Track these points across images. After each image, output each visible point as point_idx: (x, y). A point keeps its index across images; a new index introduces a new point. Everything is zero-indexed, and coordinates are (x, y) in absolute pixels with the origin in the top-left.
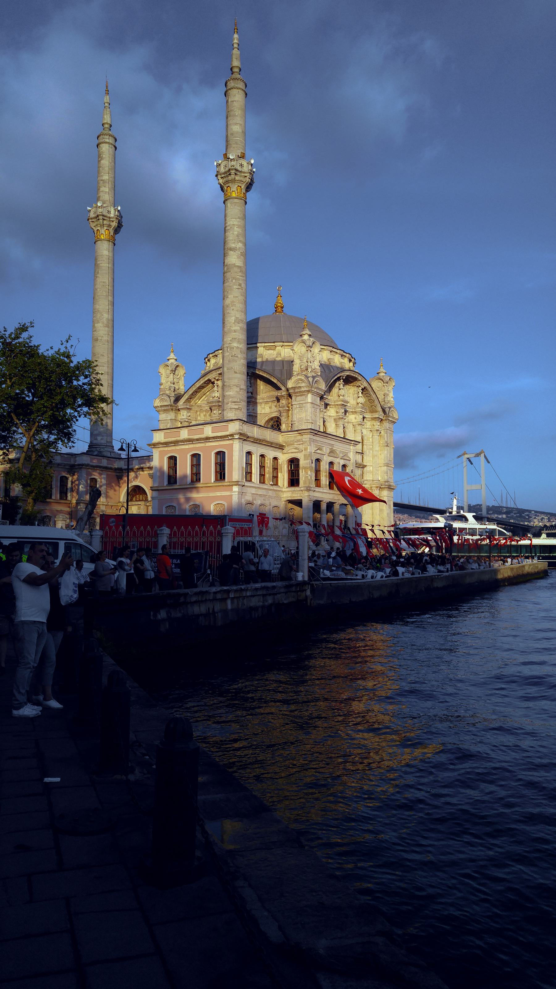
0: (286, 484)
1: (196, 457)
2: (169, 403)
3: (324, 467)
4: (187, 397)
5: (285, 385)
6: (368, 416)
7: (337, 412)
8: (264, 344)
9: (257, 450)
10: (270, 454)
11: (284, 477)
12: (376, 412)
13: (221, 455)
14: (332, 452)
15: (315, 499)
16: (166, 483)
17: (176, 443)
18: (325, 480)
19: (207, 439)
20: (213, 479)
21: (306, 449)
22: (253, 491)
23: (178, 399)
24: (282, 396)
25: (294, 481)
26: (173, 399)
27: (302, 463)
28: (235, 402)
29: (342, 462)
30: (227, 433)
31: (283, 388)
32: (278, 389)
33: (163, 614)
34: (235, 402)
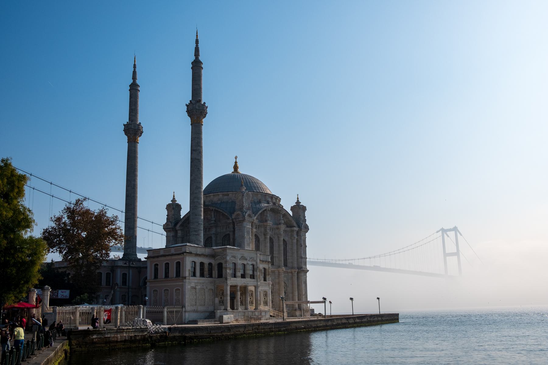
0: (216, 276)
1: (167, 265)
5: (231, 216)
6: (288, 229)
9: (198, 260)
10: (206, 261)
11: (215, 273)
13: (178, 264)
14: (243, 258)
16: (153, 277)
17: (158, 257)
19: (172, 255)
20: (175, 276)
21: (226, 258)
22: (196, 281)
23: (176, 224)
24: (230, 223)
25: (220, 275)
26: (173, 224)
27: (224, 265)
29: (250, 263)
30: (181, 252)
32: (229, 219)
33: (95, 337)
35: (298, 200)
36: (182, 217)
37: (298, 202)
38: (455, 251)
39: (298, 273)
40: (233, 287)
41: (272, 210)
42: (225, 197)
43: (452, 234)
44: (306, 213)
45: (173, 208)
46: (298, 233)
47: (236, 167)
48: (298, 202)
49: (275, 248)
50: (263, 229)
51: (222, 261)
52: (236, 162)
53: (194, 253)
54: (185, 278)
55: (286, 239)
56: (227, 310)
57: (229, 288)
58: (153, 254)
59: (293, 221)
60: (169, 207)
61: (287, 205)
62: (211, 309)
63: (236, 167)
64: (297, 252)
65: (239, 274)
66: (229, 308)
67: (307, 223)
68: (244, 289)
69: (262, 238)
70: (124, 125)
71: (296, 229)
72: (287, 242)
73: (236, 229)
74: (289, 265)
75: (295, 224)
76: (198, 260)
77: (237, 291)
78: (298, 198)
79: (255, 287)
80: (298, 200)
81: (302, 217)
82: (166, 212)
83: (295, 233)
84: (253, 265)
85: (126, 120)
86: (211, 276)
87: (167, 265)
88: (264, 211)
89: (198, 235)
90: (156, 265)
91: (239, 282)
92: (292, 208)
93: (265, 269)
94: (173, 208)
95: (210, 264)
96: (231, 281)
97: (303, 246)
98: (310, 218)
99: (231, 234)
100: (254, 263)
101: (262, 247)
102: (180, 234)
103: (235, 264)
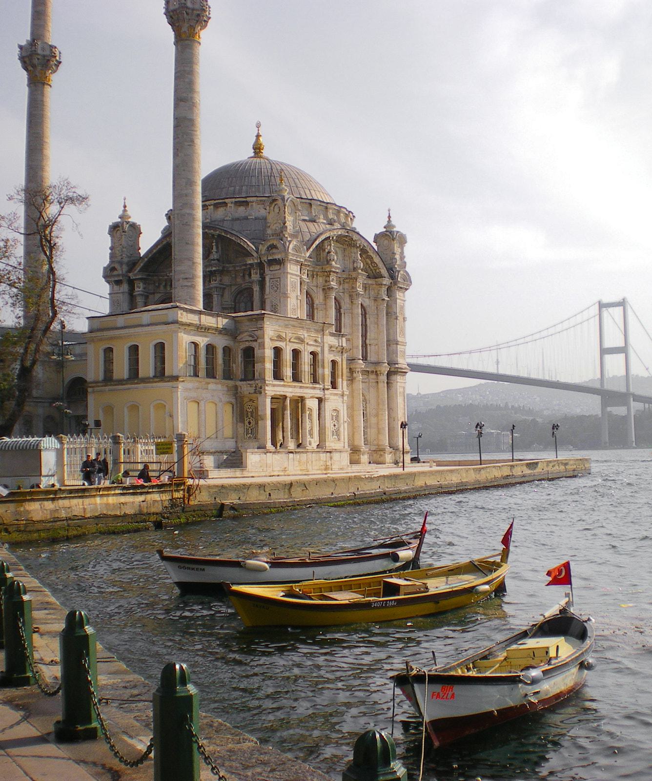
2: (120, 272)
3: (288, 357)
4: (142, 265)
6: (370, 282)
7: (326, 281)
8: (233, 200)
10: (221, 342)
11: (238, 366)
12: (382, 277)
13: (160, 348)
15: (273, 394)
16: (101, 377)
18: (288, 372)
27: (257, 352)
28: (186, 279)
29: (311, 349)
31: (255, 254)
34: (186, 279)
35: (389, 221)
36: (143, 252)
37: (389, 226)
38: (621, 344)
39: (390, 374)
40: (279, 400)
41: (340, 239)
42: (242, 209)
43: (618, 311)
44: (407, 249)
45: (124, 231)
46: (390, 291)
47: (258, 149)
48: (389, 226)
49: (346, 320)
50: (321, 280)
51: (254, 344)
52: (258, 136)
53: (192, 326)
54: (176, 378)
55: (367, 302)
56: (265, 447)
57: (268, 401)
58: (98, 325)
59: (381, 265)
60: (115, 229)
61: (368, 228)
62: (230, 445)
63: (258, 149)
64: (388, 330)
65: (288, 372)
66: (269, 445)
67: (407, 269)
68: (299, 402)
69: (319, 299)
70: (21, 47)
71: (387, 281)
72: (368, 310)
73: (267, 279)
74: (372, 357)
75: (384, 271)
76: (203, 341)
77: (284, 408)
78: (389, 217)
79: (320, 400)
80: (389, 221)
81: (397, 257)
82: (107, 241)
83: (384, 290)
84: (313, 354)
85: (25, 37)
86: (228, 375)
87: (134, 350)
88: (323, 241)
89: (193, 286)
90: (110, 350)
91: (290, 390)
92: (377, 238)
93: (334, 363)
94: (124, 231)
95: (227, 350)
96: (273, 388)
97: (400, 318)
98: (414, 257)
99: (256, 288)
100: (319, 349)
101: (319, 316)
102: (139, 288)
103: (278, 351)
